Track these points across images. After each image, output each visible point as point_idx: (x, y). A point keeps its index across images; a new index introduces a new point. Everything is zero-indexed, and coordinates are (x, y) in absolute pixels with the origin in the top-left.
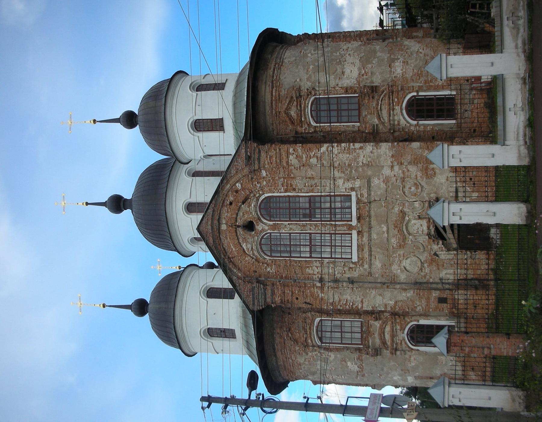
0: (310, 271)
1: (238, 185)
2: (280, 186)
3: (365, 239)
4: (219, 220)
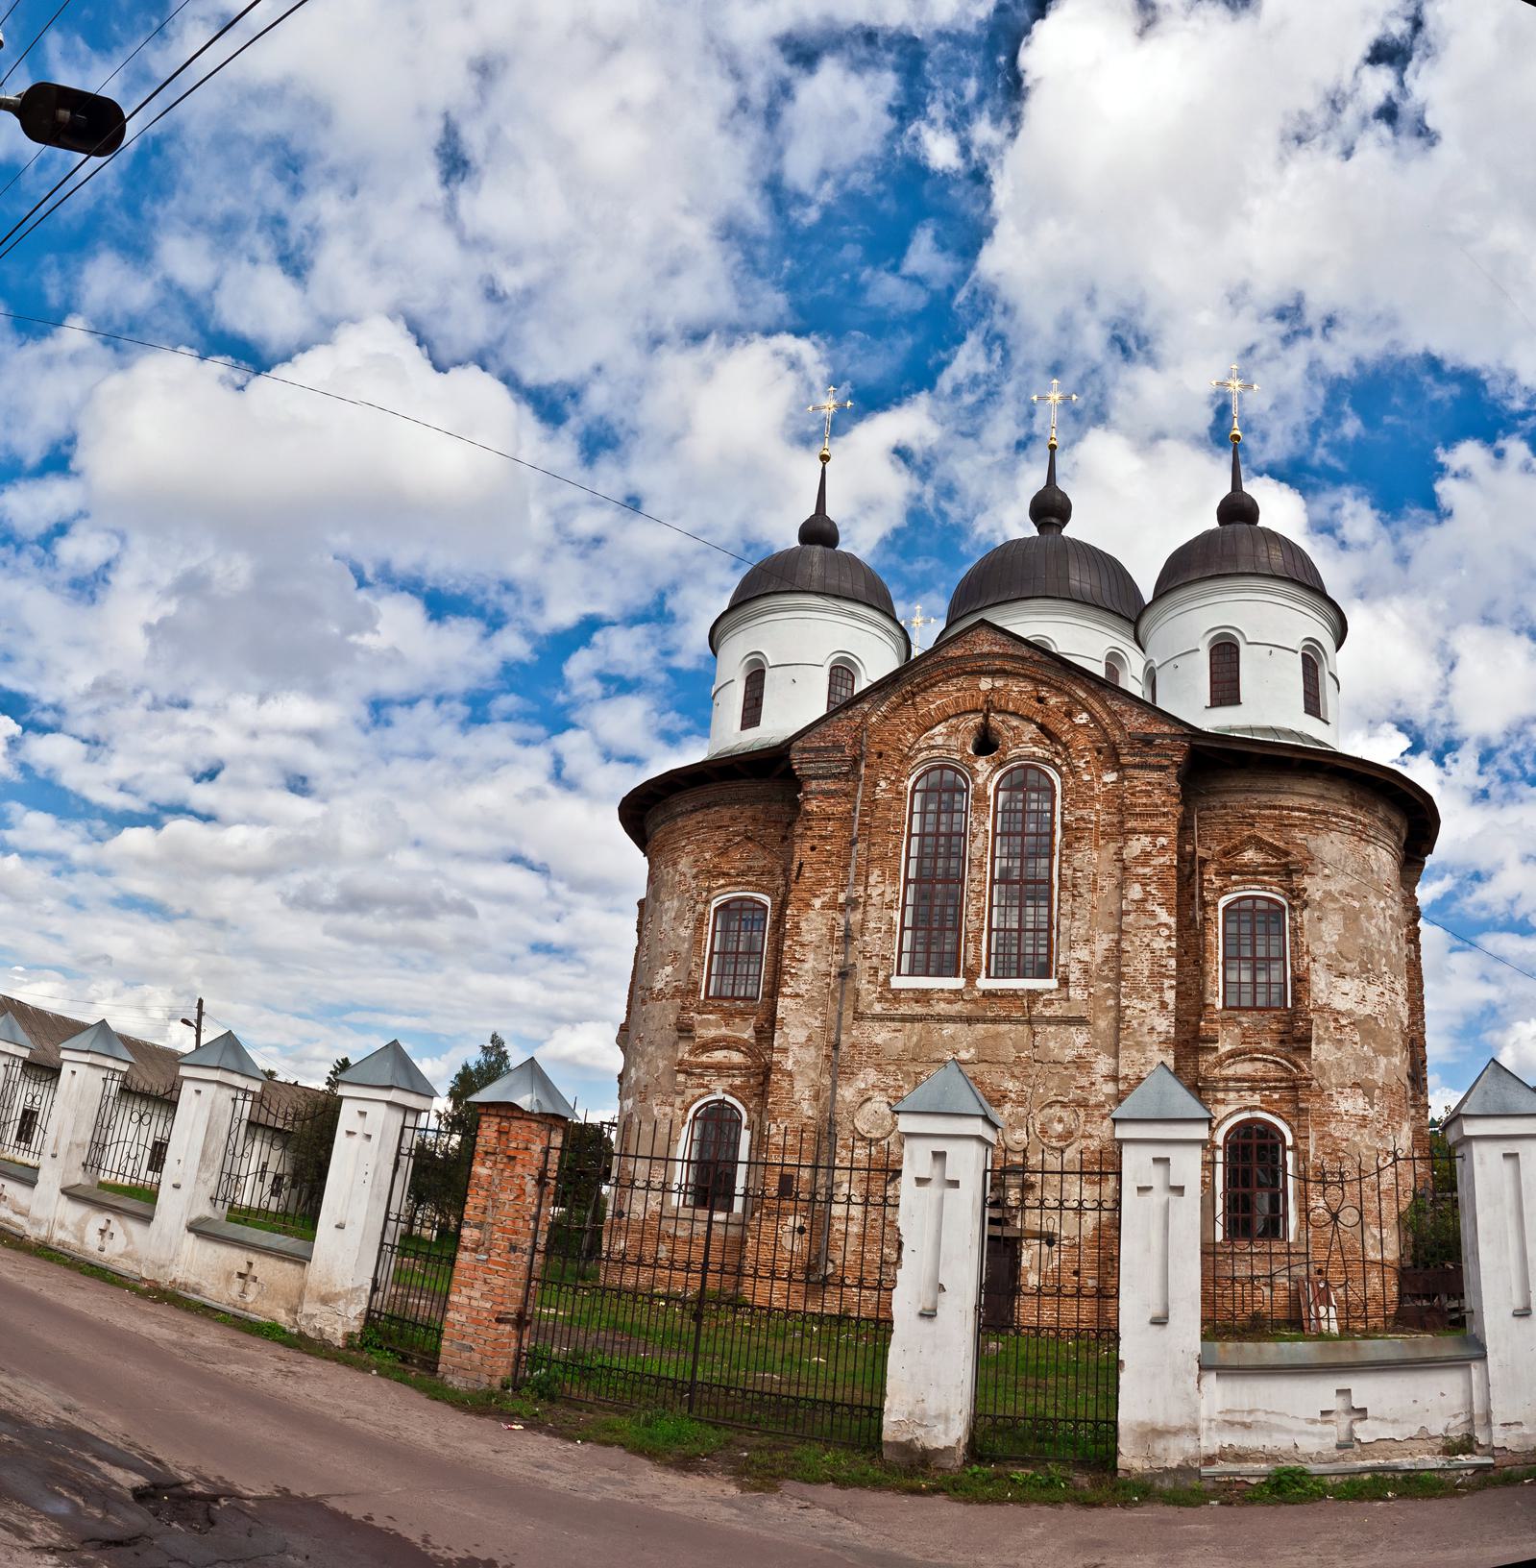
0: (872, 880)
1: (1082, 718)
2: (1079, 813)
3: (941, 1008)
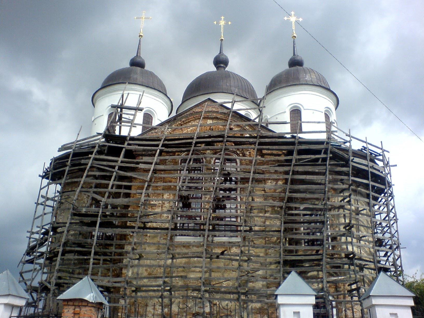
4: (216, 118)
